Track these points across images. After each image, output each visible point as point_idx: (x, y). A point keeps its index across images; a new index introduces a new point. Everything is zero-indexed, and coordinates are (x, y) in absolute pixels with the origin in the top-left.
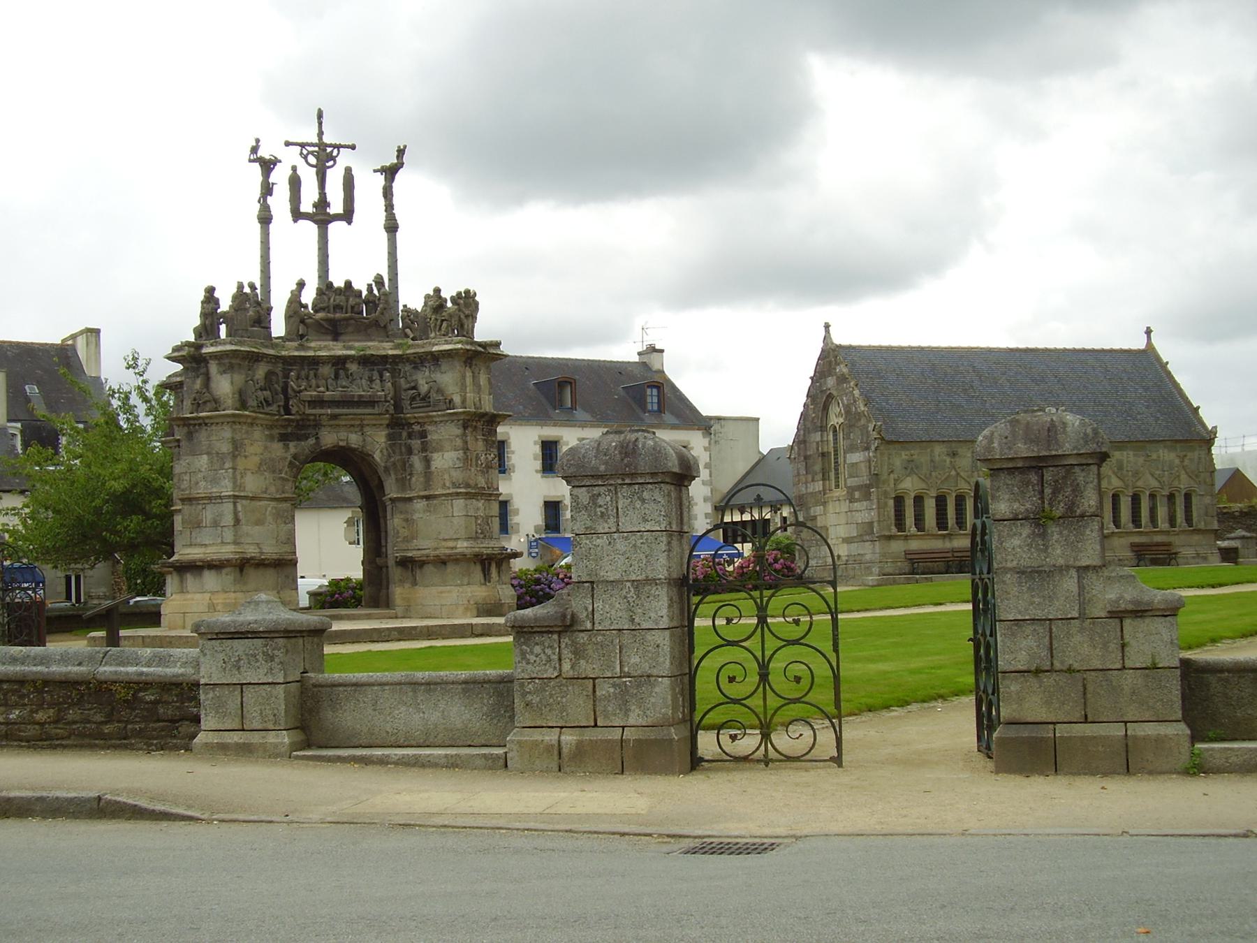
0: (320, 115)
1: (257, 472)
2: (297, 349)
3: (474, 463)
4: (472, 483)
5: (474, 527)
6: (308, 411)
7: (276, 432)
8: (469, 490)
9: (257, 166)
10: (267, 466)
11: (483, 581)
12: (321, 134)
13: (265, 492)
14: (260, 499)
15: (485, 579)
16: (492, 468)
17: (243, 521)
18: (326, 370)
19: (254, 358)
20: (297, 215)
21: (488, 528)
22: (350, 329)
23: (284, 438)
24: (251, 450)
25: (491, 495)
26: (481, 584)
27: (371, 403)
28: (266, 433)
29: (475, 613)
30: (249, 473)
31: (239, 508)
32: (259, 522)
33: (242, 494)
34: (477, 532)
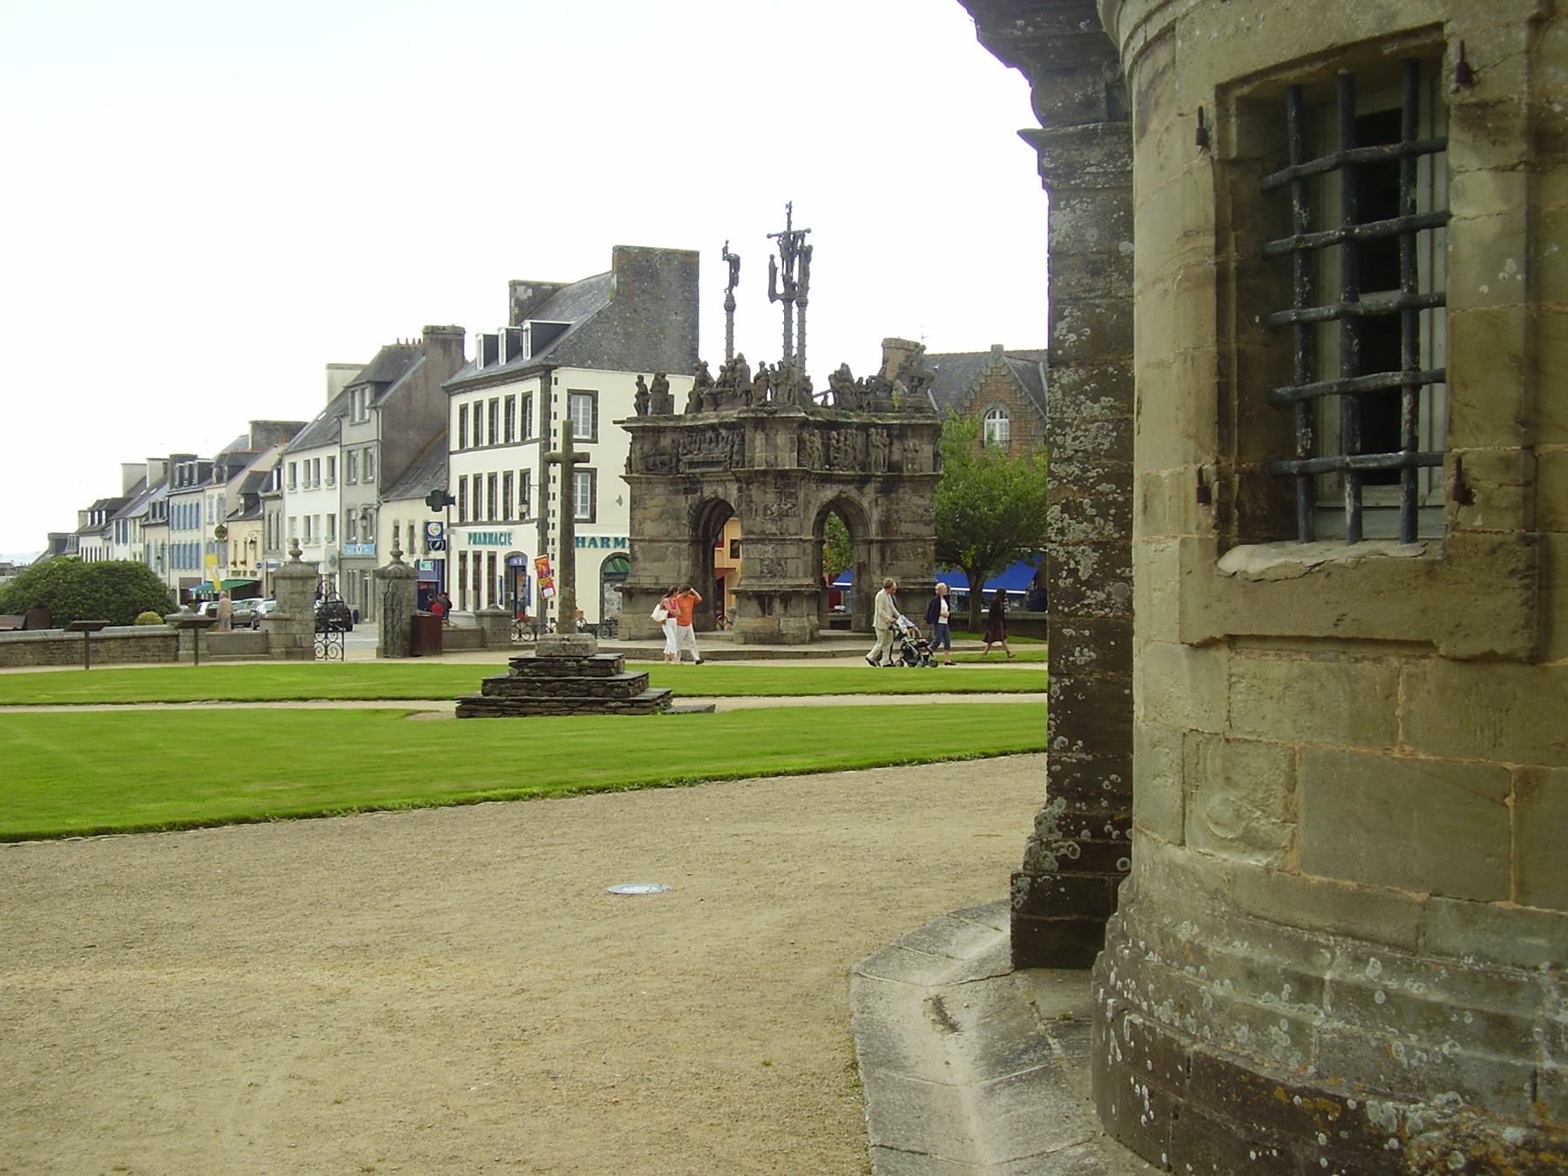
0: (789, 206)
1: (657, 520)
2: (691, 420)
3: (761, 512)
4: (755, 530)
5: (759, 568)
6: (688, 471)
7: (682, 487)
8: (752, 537)
9: (727, 264)
10: (665, 514)
11: (760, 614)
12: (789, 223)
13: (667, 536)
14: (661, 541)
15: (764, 612)
16: (787, 516)
17: (641, 559)
18: (709, 434)
19: (660, 431)
20: (773, 296)
21: (780, 568)
22: (724, 401)
23: (686, 492)
24: (649, 503)
25: (784, 540)
26: (758, 617)
27: (718, 463)
28: (671, 488)
29: (742, 640)
30: (648, 522)
31: (636, 548)
32: (661, 559)
33: (639, 538)
34: (762, 572)
